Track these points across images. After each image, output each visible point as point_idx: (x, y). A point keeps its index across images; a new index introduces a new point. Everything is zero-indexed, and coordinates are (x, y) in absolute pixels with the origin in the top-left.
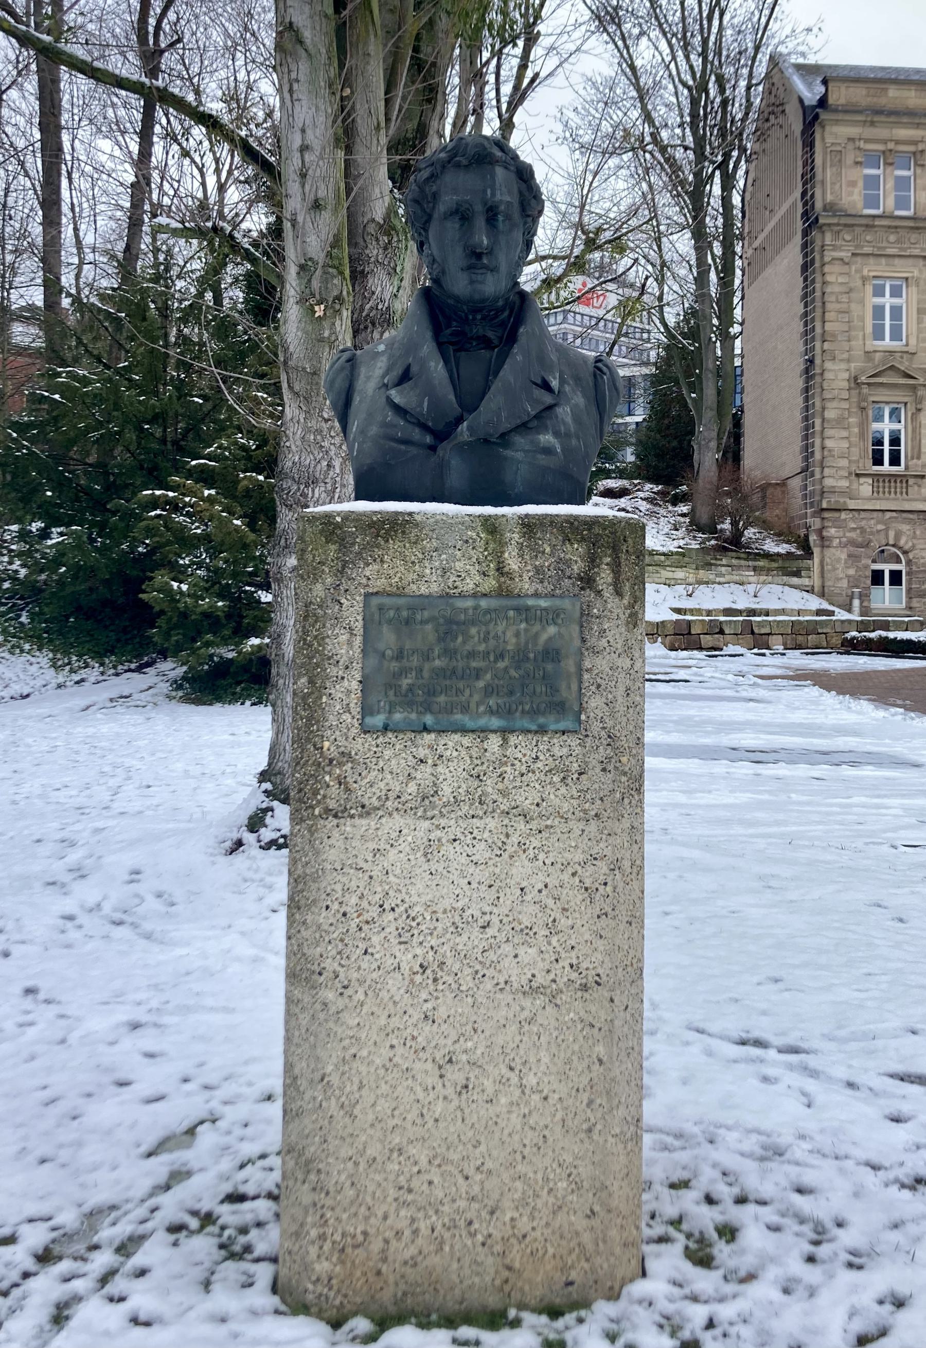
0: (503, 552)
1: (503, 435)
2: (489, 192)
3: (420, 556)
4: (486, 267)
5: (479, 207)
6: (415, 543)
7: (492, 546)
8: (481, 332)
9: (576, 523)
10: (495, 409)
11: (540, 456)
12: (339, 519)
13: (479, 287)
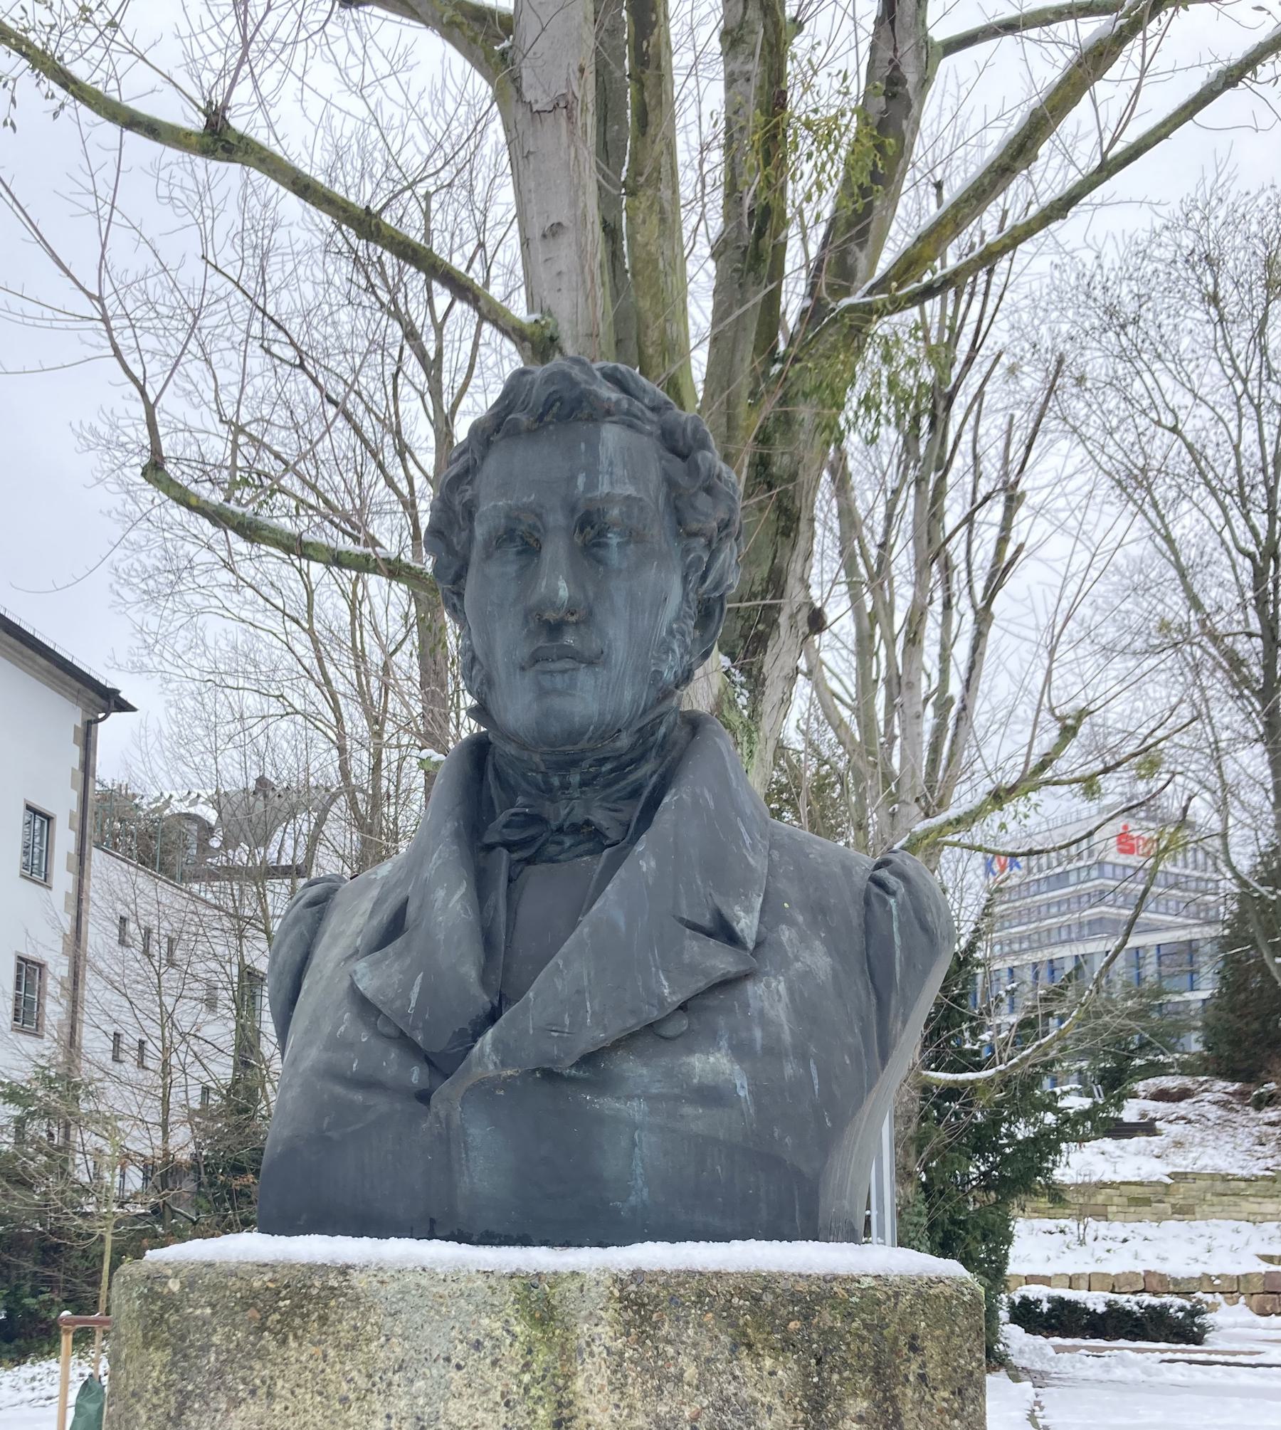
0: (569, 1377)
1: (589, 1059)
2: (581, 480)
3: (362, 1382)
4: (575, 656)
5: (557, 519)
6: (348, 1347)
7: (542, 1357)
8: (579, 816)
9: (768, 1299)
10: (570, 993)
11: (688, 1110)
12: (174, 1286)
13: (557, 703)
